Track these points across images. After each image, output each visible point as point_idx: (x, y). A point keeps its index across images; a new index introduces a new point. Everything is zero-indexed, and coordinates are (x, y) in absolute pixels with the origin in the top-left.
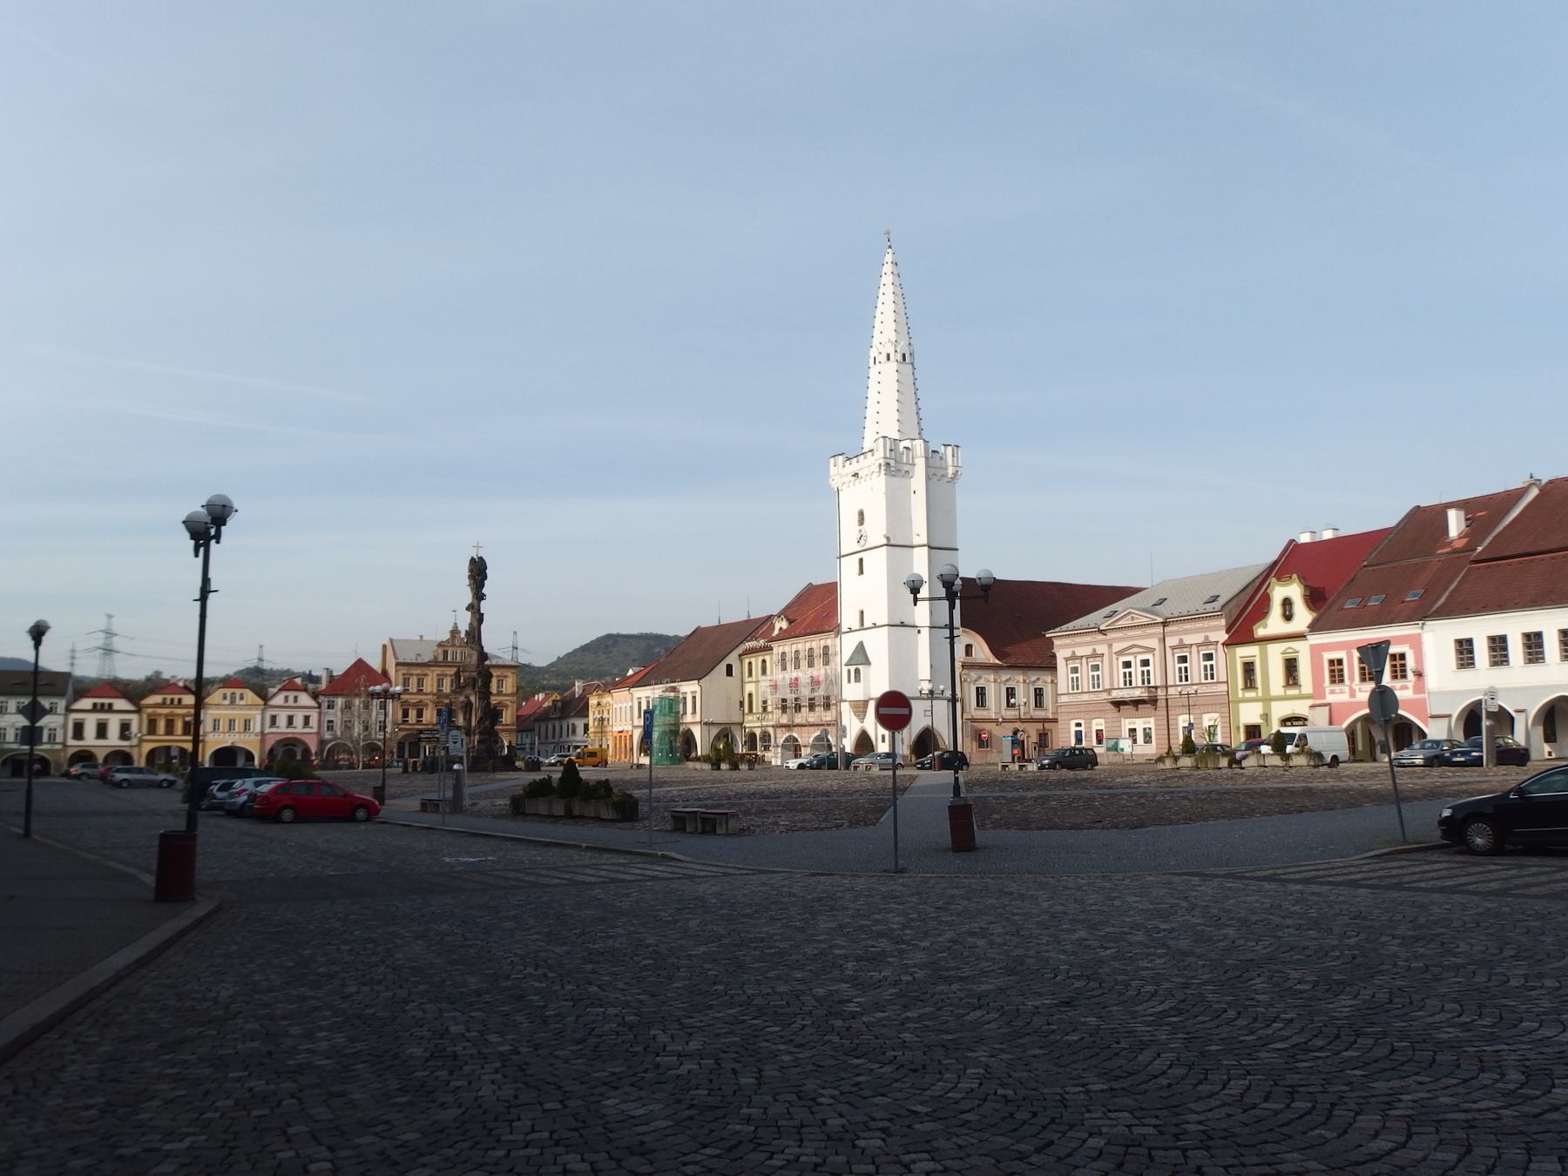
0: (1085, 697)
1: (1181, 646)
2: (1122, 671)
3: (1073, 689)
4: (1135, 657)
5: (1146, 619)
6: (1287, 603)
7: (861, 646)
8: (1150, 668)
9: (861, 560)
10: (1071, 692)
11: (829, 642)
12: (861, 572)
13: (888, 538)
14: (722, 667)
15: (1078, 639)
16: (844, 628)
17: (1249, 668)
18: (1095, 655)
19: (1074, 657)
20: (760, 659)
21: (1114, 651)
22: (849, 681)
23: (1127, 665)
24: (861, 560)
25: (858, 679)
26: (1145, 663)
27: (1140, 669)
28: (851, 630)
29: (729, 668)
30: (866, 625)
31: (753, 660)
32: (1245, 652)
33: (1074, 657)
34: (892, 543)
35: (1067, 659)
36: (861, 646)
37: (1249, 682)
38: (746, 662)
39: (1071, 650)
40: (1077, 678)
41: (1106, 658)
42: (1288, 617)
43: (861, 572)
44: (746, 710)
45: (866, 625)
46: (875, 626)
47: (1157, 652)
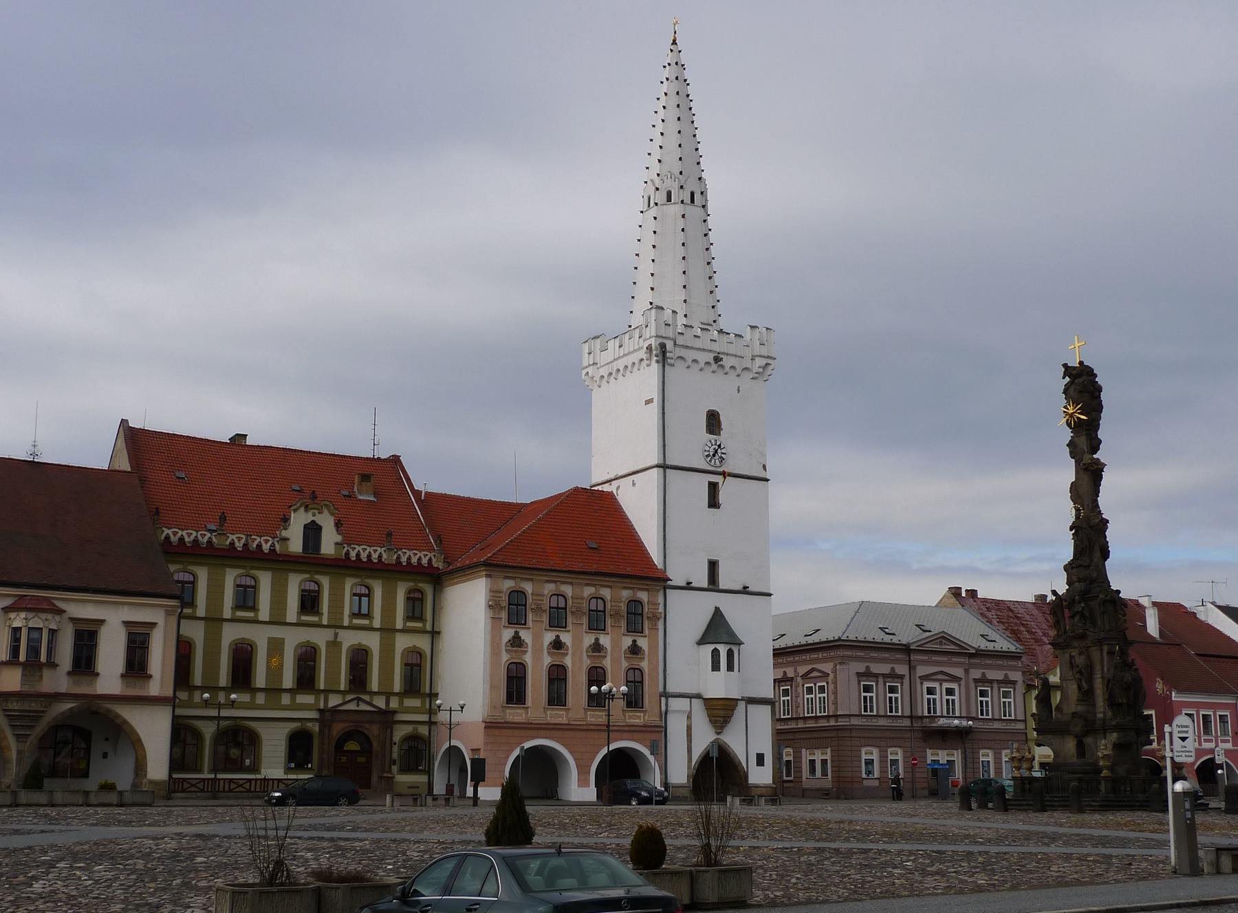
0: (882, 722)
1: (984, 680)
2: (926, 696)
3: (866, 710)
4: (941, 685)
8: (956, 698)
9: (713, 487)
11: (643, 596)
18: (893, 676)
19: (867, 674)
21: (918, 675)
23: (931, 691)
24: (713, 487)
26: (950, 692)
28: (688, 587)
35: (859, 674)
40: (812, 698)
41: (906, 681)
47: (963, 683)
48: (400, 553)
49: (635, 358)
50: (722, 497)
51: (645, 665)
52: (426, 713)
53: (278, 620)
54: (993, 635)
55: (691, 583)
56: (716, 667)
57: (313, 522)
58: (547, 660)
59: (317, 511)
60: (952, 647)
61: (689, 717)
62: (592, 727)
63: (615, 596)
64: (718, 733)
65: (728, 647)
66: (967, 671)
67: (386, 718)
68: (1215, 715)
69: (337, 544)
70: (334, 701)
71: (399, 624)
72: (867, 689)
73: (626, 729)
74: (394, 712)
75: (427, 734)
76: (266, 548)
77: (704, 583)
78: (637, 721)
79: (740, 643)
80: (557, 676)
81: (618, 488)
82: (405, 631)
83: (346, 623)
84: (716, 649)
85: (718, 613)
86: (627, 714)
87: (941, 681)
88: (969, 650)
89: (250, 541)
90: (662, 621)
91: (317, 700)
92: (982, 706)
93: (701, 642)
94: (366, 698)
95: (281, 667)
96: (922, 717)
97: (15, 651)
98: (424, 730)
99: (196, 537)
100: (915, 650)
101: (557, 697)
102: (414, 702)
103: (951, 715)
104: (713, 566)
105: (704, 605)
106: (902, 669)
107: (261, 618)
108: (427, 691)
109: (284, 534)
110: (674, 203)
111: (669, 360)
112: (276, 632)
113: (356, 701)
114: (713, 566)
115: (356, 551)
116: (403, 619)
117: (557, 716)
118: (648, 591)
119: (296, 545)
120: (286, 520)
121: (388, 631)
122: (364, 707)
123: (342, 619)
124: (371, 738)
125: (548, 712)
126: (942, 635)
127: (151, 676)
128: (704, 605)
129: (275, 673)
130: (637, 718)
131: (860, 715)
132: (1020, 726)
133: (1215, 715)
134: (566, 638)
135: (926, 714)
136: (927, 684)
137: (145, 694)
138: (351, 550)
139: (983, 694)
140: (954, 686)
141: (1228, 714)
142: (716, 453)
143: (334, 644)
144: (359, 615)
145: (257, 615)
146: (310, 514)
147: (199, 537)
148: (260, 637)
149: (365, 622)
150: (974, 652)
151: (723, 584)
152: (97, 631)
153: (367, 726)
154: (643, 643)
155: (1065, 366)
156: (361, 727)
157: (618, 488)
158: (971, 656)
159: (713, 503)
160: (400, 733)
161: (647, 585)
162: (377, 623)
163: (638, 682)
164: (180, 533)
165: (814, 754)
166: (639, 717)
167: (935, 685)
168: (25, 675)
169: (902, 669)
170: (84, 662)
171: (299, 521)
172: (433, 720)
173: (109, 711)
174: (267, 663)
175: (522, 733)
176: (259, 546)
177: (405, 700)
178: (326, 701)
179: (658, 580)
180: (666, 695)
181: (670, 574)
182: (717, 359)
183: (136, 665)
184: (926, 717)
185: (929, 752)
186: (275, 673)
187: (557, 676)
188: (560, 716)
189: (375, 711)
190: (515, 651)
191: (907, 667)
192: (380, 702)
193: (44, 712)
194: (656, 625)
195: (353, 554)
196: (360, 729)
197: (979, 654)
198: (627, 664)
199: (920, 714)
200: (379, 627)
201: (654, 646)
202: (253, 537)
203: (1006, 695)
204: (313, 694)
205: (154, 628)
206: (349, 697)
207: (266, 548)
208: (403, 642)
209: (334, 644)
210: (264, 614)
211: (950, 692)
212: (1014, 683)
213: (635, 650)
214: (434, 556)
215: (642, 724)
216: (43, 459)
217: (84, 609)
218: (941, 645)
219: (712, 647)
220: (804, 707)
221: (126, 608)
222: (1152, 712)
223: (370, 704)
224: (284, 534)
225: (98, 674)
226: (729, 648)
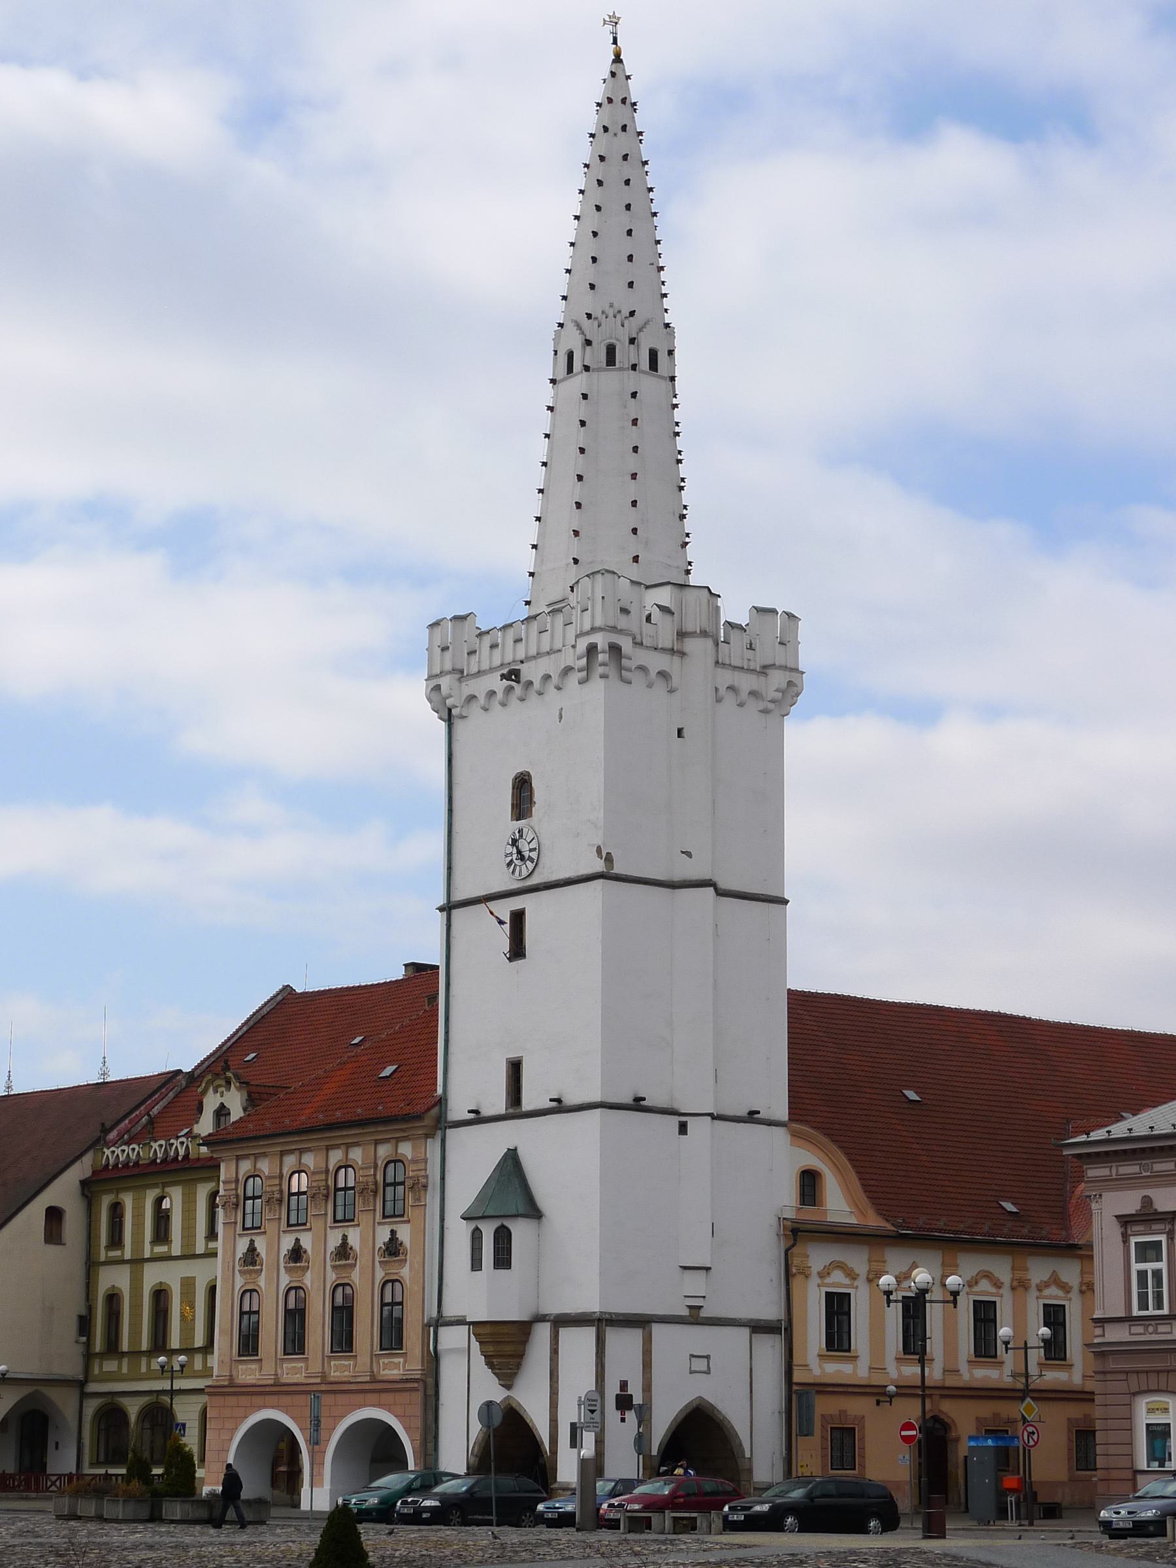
3: (1143, 1305)
7: (511, 1165)
9: (518, 918)
10: (1136, 1312)
12: (517, 951)
13: (609, 859)
14: (35, 1213)
16: (458, 1109)
20: (151, 1196)
22: (476, 1264)
25: (503, 1260)
28: (478, 1118)
29: (54, 1215)
30: (529, 1102)
31: (128, 1200)
34: (618, 869)
36: (511, 1165)
38: (106, 1201)
43: (517, 951)
44: (98, 1345)
45: (527, 1104)
46: (559, 1107)
51: (405, 1272)
53: (189, 1256)
57: (222, 1104)
64: (508, 1387)
65: (495, 1224)
76: (182, 1152)
78: (395, 1372)
84: (503, 1226)
86: (381, 1361)
103: (1151, 1312)
107: (174, 1254)
114: (515, 1068)
120: (200, 1109)
130: (393, 1368)
134: (306, 1241)
145: (170, 1249)
146: (218, 1094)
154: (404, 1234)
166: (397, 1366)
171: (211, 1102)
188: (297, 1371)
190: (250, 1272)
198: (383, 1274)
201: (420, 1234)
202: (172, 1141)
213: (393, 1248)
215: (398, 1377)
216: (115, 1075)
226: (473, 1226)
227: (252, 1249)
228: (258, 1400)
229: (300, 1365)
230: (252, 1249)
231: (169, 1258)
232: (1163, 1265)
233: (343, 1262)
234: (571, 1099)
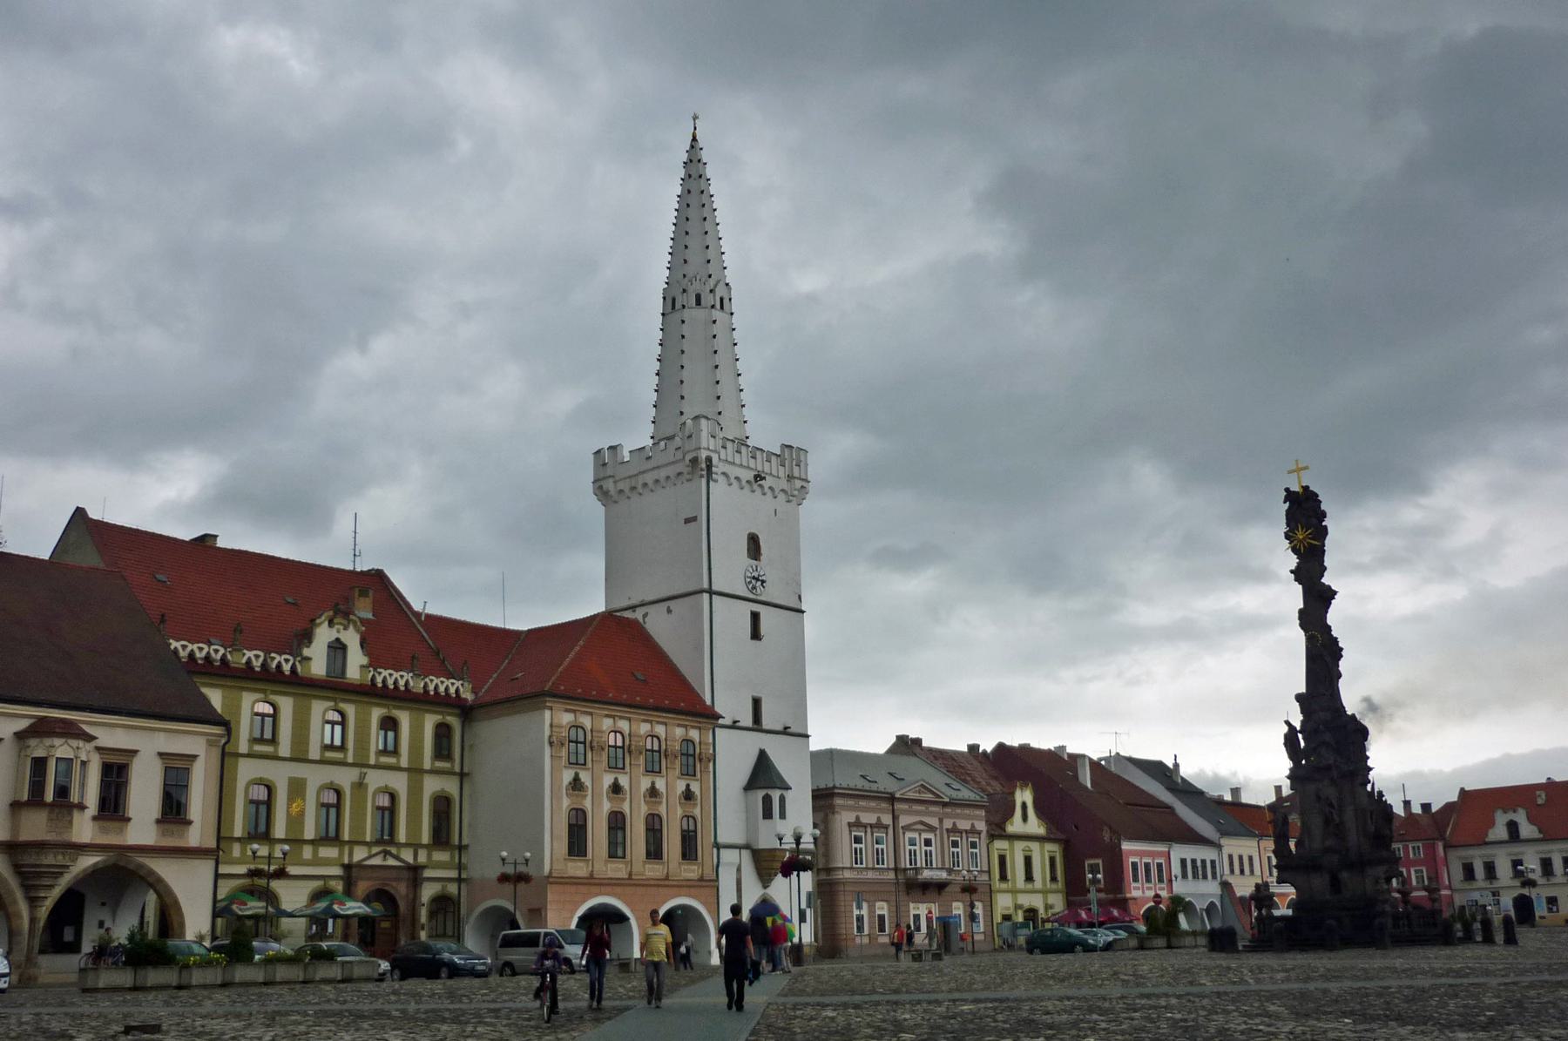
0: (870, 875)
1: (954, 830)
4: (920, 835)
5: (931, 796)
6: (1024, 806)
8: (932, 849)
9: (755, 617)
11: (694, 734)
15: (863, 803)
17: (1002, 859)
18: (879, 826)
24: (755, 617)
25: (783, 816)
26: (928, 843)
27: (924, 848)
28: (734, 726)
32: (1000, 845)
33: (857, 824)
35: (850, 825)
37: (1003, 877)
39: (857, 814)
42: (1025, 818)
47: (938, 832)
48: (427, 680)
49: (671, 471)
50: (764, 629)
52: (455, 869)
53: (299, 757)
54: (956, 785)
55: (739, 721)
56: (768, 814)
57: (338, 640)
58: (607, 806)
59: (341, 627)
60: (929, 796)
61: (739, 870)
62: (652, 882)
63: (673, 732)
64: (765, 887)
66: (941, 821)
67: (414, 874)
68: (1141, 862)
69: (362, 667)
70: (359, 854)
71: (427, 765)
72: (858, 840)
73: (684, 883)
74: (424, 867)
75: (456, 892)
76: (287, 668)
77: (747, 721)
79: (788, 788)
80: (617, 823)
81: (645, 616)
82: (434, 772)
83: (372, 762)
85: (762, 755)
87: (920, 832)
88: (942, 798)
89: (269, 660)
90: (711, 764)
91: (341, 854)
92: (953, 857)
93: (750, 786)
94: (394, 850)
95: (302, 814)
96: (905, 870)
97: (37, 786)
98: (452, 889)
99: (208, 653)
100: (899, 798)
101: (616, 849)
102: (441, 856)
104: (757, 703)
105: (751, 744)
106: (887, 819)
107: (281, 754)
108: (457, 843)
109: (306, 652)
110: (705, 308)
111: (713, 475)
112: (299, 770)
113: (382, 855)
115: (382, 676)
116: (431, 758)
117: (617, 870)
118: (700, 728)
119: (318, 665)
121: (415, 771)
122: (391, 862)
123: (368, 757)
124: (398, 898)
125: (609, 865)
126: (922, 783)
127: (190, 823)
128: (751, 744)
129: (296, 821)
131: (852, 868)
132: (985, 877)
133: (1141, 862)
135: (908, 866)
136: (909, 835)
137: (122, 843)
138: (377, 675)
139: (955, 844)
140: (930, 836)
141: (1100, 861)
142: (757, 580)
143: (360, 786)
144: (385, 752)
145: (276, 750)
146: (334, 630)
147: (212, 652)
148: (280, 775)
149: (392, 760)
150: (948, 800)
151: (767, 723)
152: (128, 765)
153: (394, 884)
154: (695, 787)
155: (1287, 490)
156: (387, 885)
157: (645, 616)
158: (945, 805)
159: (756, 635)
160: (428, 892)
161: (700, 722)
162: (404, 763)
163: (692, 831)
164: (190, 647)
165: (918, 908)
166: (693, 871)
167: (916, 835)
168: (52, 820)
169: (887, 819)
170: (112, 806)
171: (324, 635)
172: (464, 876)
173: (142, 866)
174: (288, 808)
175: (583, 889)
176: (279, 666)
177: (434, 853)
178: (351, 854)
179: (708, 716)
180: (718, 846)
181: (718, 709)
182: (759, 477)
183: (173, 809)
184: (910, 869)
185: (912, 905)
186: (296, 821)
187: (617, 823)
189: (400, 866)
190: (577, 796)
191: (891, 816)
192: (407, 856)
193: (68, 867)
194: (707, 767)
195: (379, 680)
196: (386, 888)
197: (953, 804)
199: (903, 866)
200: (406, 766)
202: (273, 655)
203: (974, 845)
204: (266, 845)
205: (193, 761)
206: (375, 850)
207: (287, 668)
208: (432, 785)
209: (360, 786)
210: (285, 749)
211: (928, 843)
212: (979, 833)
213: (688, 795)
214: (462, 685)
217: (113, 734)
218: (919, 793)
219: (761, 794)
220: (887, 856)
221: (162, 734)
222: (1100, 861)
223: (397, 858)
224: (306, 652)
225: (129, 819)
227: (576, 779)
228: (594, 889)
229: (621, 866)
230: (576, 779)
231: (275, 757)
232: (884, 847)
233: (653, 799)
234: (793, 730)
